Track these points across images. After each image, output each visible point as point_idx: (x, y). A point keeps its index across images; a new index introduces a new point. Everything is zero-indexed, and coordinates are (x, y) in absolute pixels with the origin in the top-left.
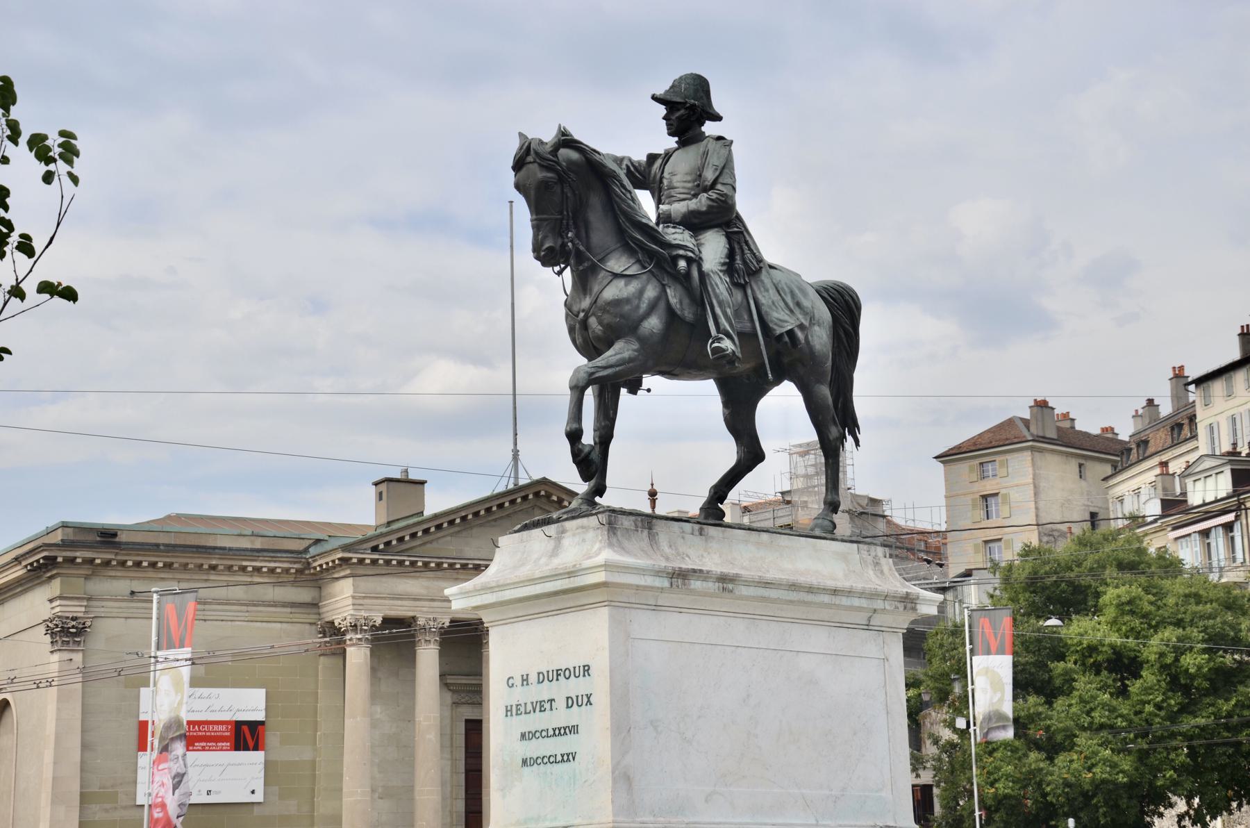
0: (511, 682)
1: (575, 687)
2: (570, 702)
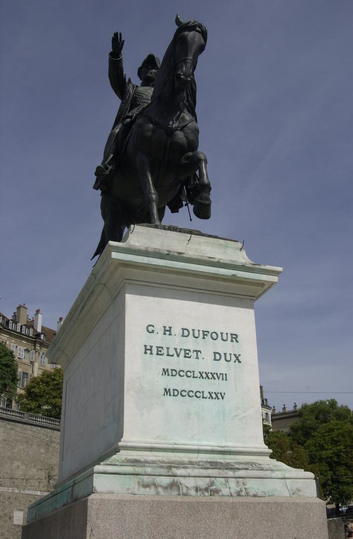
0: (151, 329)
1: (222, 347)
2: (217, 356)
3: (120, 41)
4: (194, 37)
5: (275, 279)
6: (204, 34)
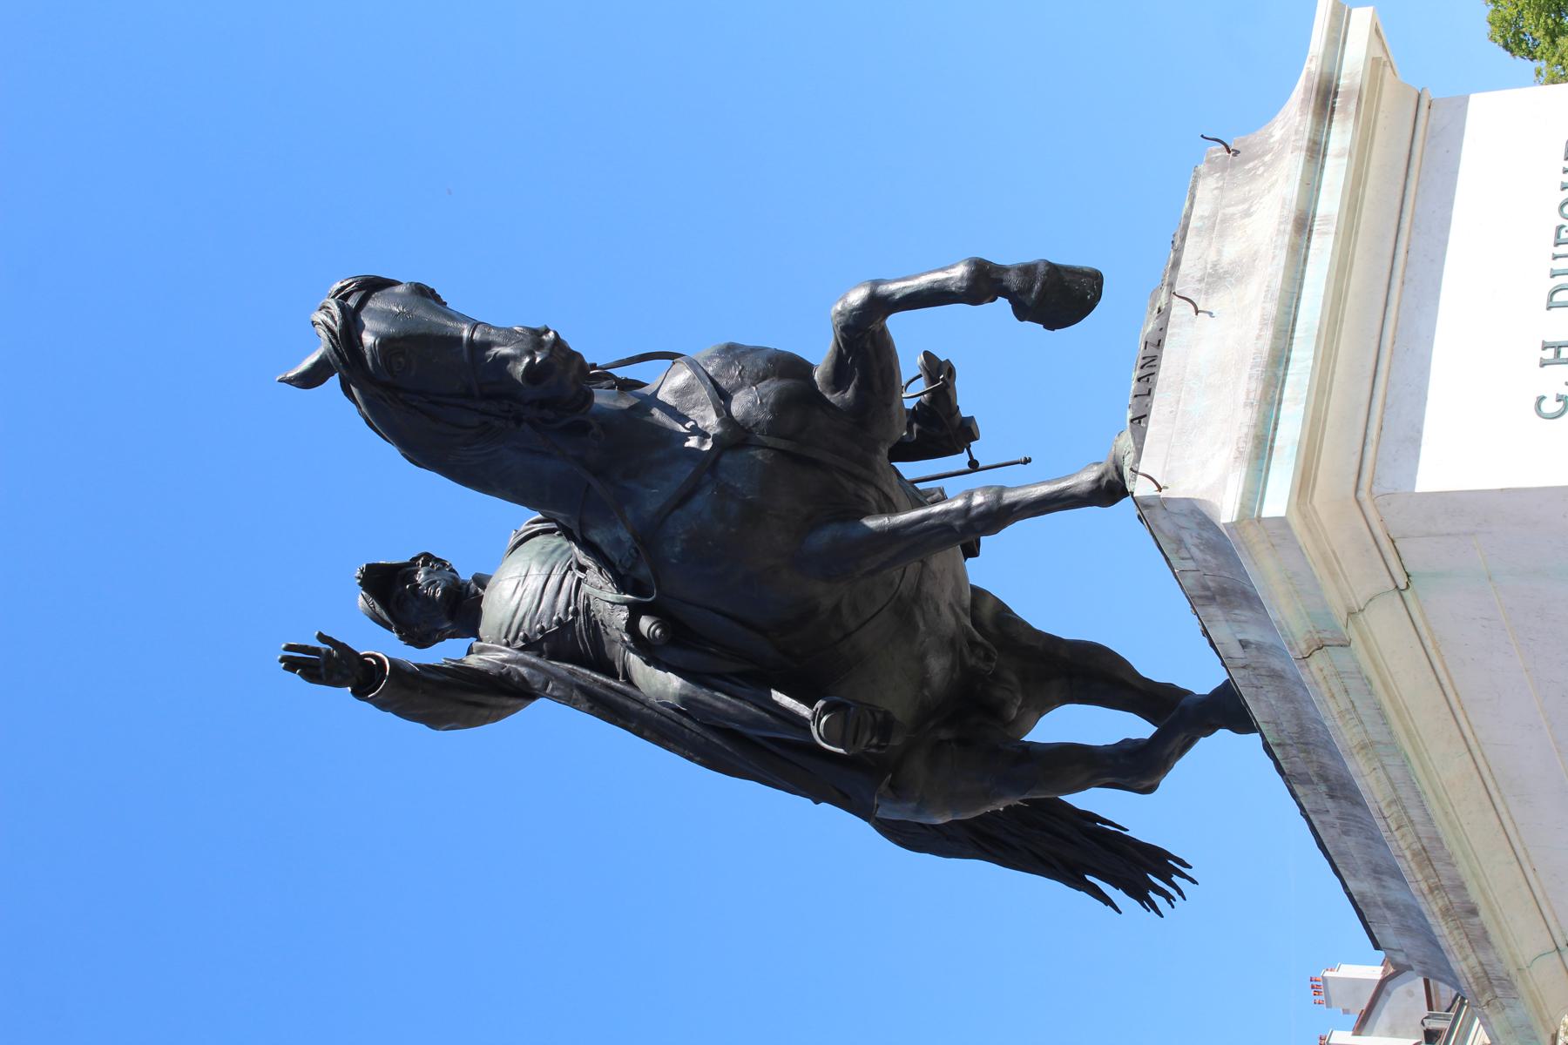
0: (1550, 406)
3: (316, 651)
4: (386, 315)
5: (1361, 21)
6: (372, 286)
